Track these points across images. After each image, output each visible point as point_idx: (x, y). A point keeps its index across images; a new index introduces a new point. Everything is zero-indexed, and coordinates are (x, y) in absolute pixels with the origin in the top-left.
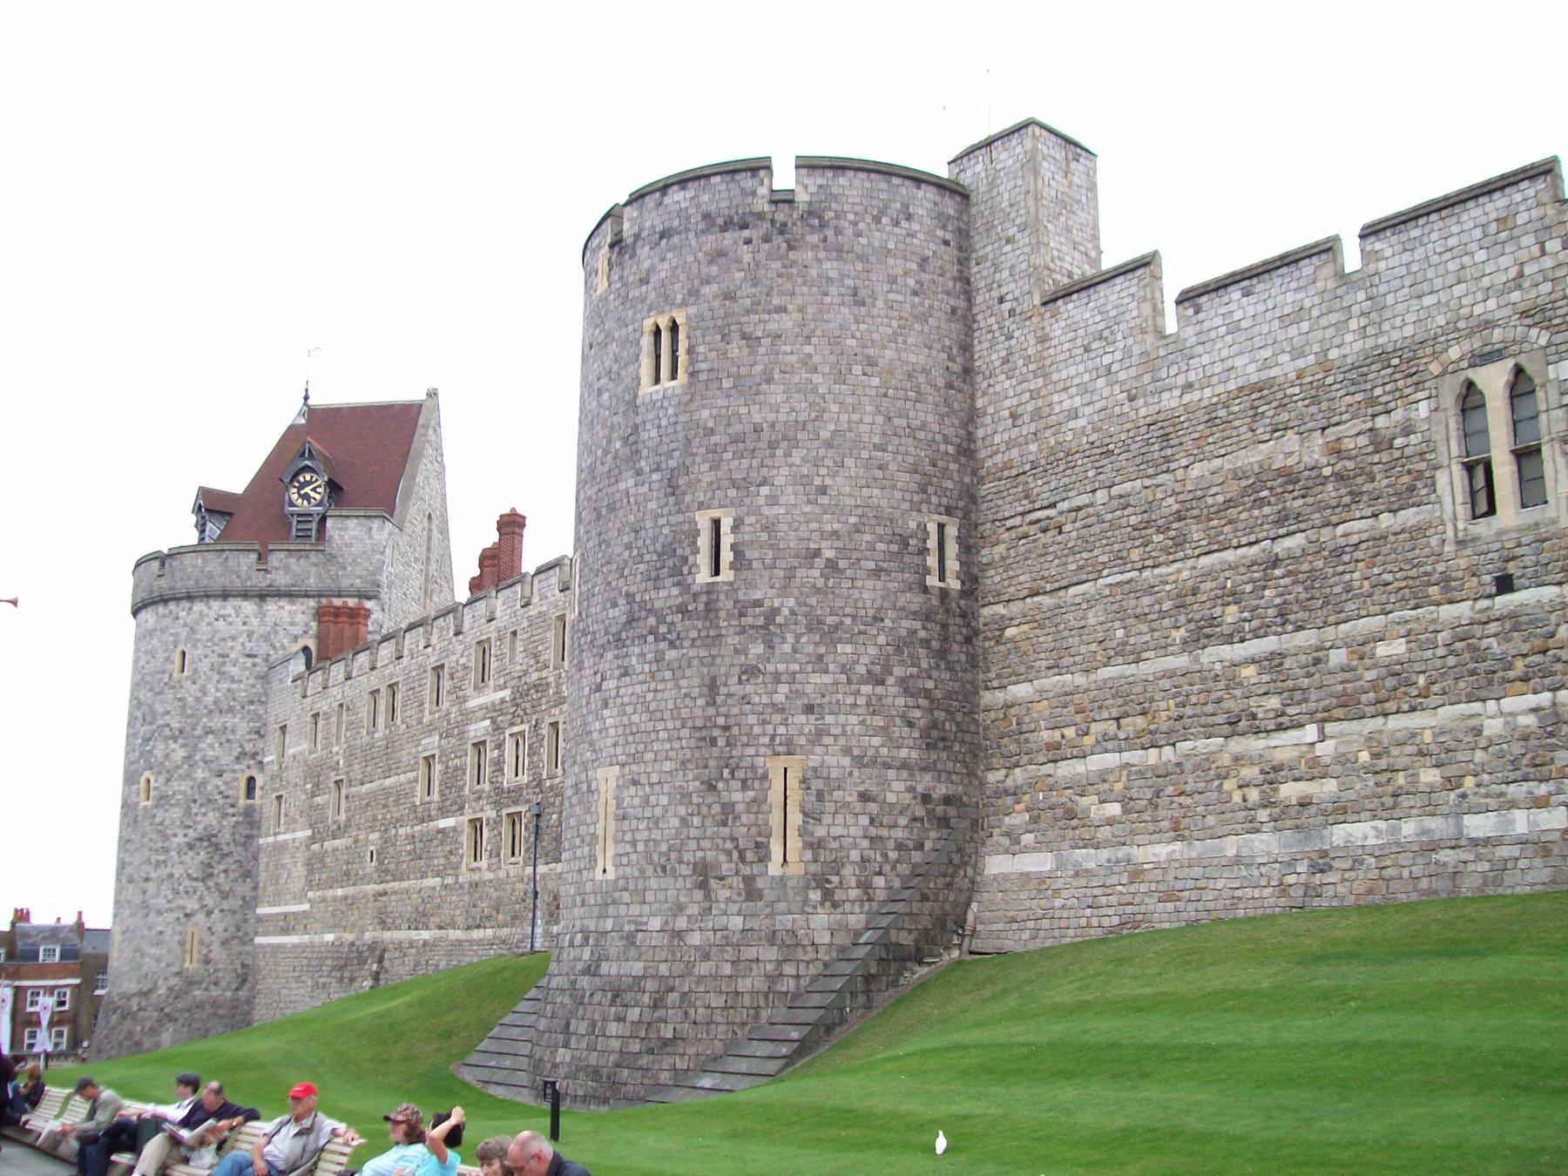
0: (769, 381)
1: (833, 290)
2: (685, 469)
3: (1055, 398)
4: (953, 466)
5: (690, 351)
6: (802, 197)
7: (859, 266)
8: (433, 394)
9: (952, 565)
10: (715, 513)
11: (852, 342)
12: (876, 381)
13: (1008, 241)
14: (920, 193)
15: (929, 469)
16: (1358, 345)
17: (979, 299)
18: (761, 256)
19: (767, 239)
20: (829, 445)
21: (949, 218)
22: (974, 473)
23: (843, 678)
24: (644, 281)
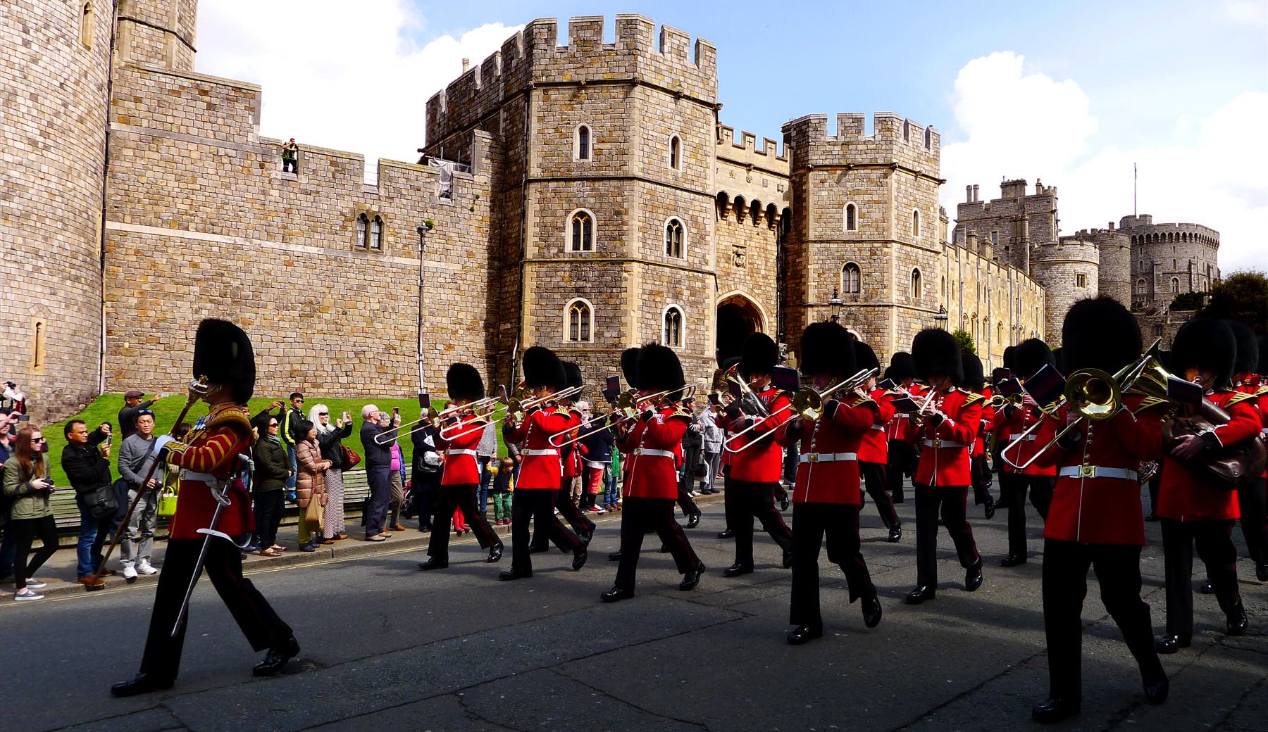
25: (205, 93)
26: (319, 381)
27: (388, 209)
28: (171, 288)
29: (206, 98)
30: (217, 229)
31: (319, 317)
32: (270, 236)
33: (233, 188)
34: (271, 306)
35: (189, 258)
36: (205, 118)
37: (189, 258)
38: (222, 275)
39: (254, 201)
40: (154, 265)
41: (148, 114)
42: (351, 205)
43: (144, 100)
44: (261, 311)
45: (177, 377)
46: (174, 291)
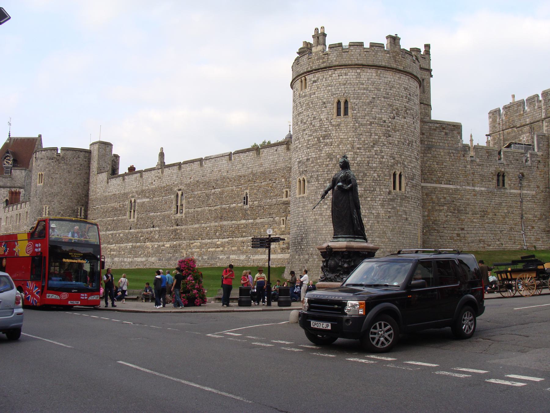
0: (55, 185)
1: (65, 170)
2: (42, 198)
3: (97, 189)
4: (84, 198)
5: (44, 179)
6: (61, 155)
7: (70, 166)
8: (40, 136)
9: (83, 214)
10: (46, 206)
11: (67, 179)
12: (71, 185)
13: (95, 162)
14: (81, 153)
15: (79, 199)
16: (123, 191)
17: (91, 170)
18: (55, 165)
19: (56, 162)
20: (63, 196)
21: (87, 156)
22: (88, 199)
23: (63, 232)
24: (39, 166)
25: (444, 128)
26: (490, 243)
27: (507, 170)
28: (437, 208)
29: (444, 131)
30: (451, 183)
31: (487, 217)
32: (468, 184)
33: (455, 166)
34: (470, 213)
35: (442, 195)
36: (445, 139)
37: (442, 195)
38: (453, 201)
39: (462, 170)
40: (432, 198)
41: (427, 139)
42: (494, 169)
43: (425, 134)
44: (467, 215)
45: (442, 243)
46: (439, 209)
